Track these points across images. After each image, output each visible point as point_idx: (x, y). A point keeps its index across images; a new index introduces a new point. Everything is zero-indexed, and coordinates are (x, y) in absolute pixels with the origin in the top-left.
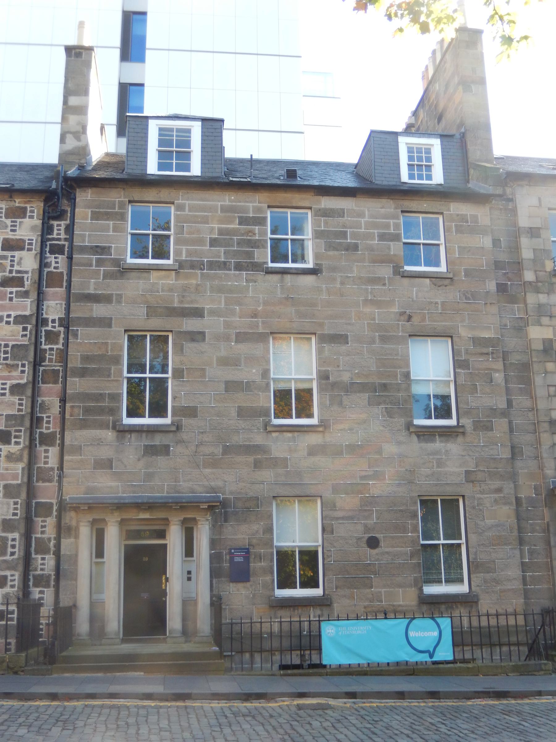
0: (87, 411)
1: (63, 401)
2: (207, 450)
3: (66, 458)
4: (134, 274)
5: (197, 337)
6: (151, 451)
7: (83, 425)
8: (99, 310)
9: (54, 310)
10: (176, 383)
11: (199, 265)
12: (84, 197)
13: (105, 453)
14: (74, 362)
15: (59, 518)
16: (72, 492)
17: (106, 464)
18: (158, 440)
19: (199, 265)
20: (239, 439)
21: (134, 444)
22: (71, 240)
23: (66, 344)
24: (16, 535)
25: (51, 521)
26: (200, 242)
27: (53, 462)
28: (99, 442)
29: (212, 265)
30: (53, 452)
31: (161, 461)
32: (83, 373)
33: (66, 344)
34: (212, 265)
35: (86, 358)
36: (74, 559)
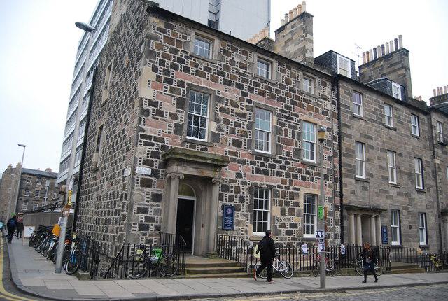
0: (348, 170)
1: (340, 166)
2: (376, 190)
3: (344, 188)
4: (356, 119)
5: (372, 147)
6: (365, 189)
7: (347, 176)
8: (349, 131)
9: (336, 129)
10: (367, 164)
11: (370, 120)
12: (343, 84)
13: (353, 187)
14: (343, 151)
15: (342, 212)
16: (345, 202)
17: (353, 192)
18: (366, 185)
19: (370, 120)
20: (382, 187)
21: (360, 185)
22: (338, 100)
23: (340, 143)
24: (332, 218)
25: (339, 213)
26: (370, 111)
27: (338, 190)
28: (351, 184)
29: (375, 121)
30: (338, 184)
31: (367, 193)
32: (346, 155)
33: (340, 143)
34: (375, 121)
35: (347, 150)
36: (349, 229)
